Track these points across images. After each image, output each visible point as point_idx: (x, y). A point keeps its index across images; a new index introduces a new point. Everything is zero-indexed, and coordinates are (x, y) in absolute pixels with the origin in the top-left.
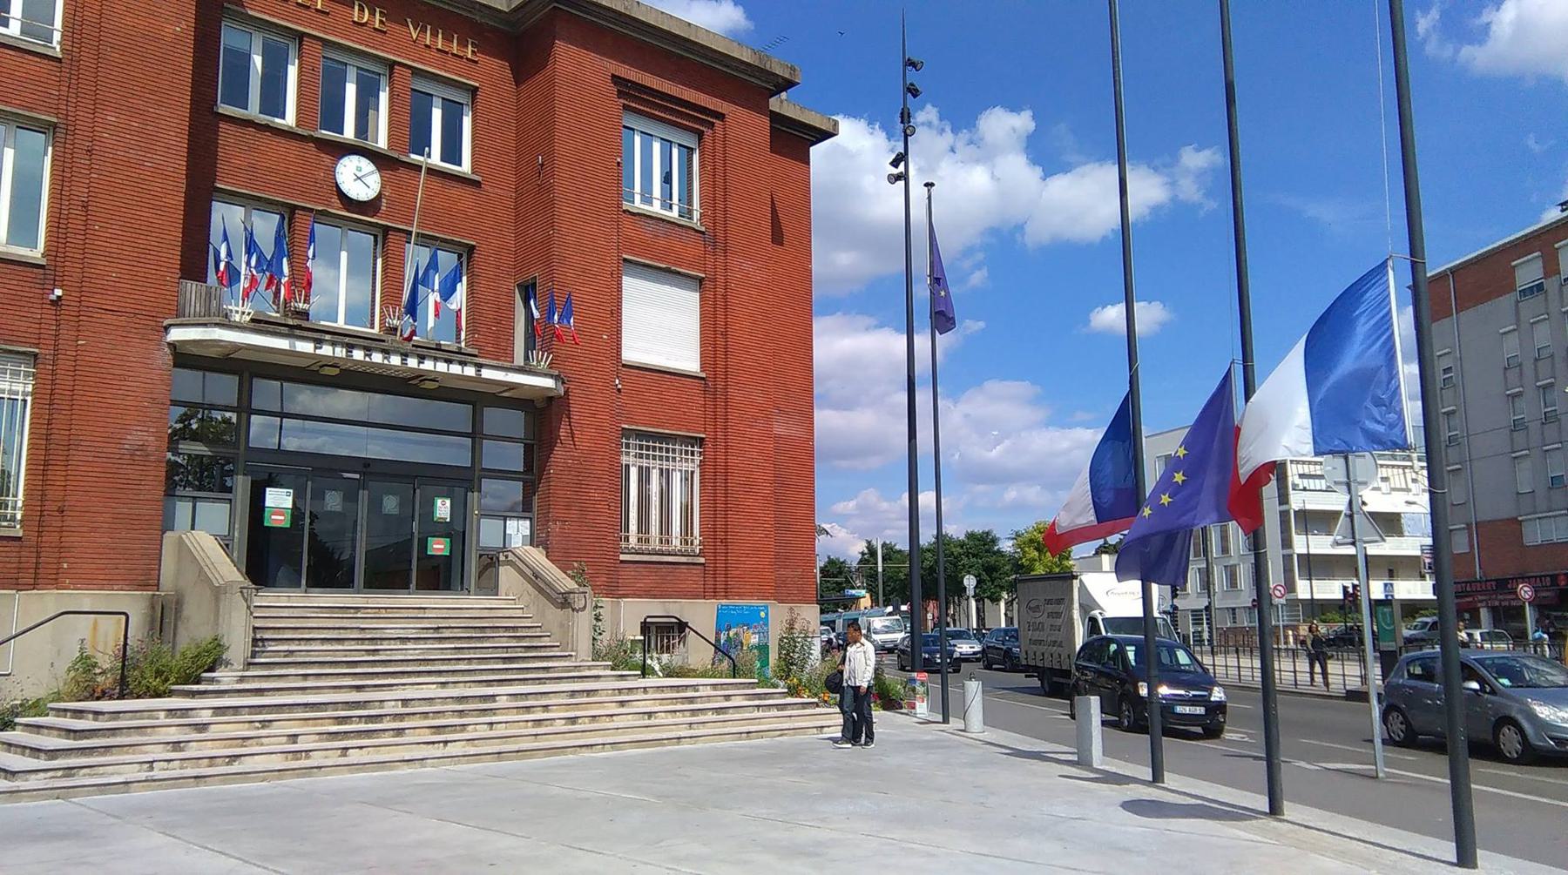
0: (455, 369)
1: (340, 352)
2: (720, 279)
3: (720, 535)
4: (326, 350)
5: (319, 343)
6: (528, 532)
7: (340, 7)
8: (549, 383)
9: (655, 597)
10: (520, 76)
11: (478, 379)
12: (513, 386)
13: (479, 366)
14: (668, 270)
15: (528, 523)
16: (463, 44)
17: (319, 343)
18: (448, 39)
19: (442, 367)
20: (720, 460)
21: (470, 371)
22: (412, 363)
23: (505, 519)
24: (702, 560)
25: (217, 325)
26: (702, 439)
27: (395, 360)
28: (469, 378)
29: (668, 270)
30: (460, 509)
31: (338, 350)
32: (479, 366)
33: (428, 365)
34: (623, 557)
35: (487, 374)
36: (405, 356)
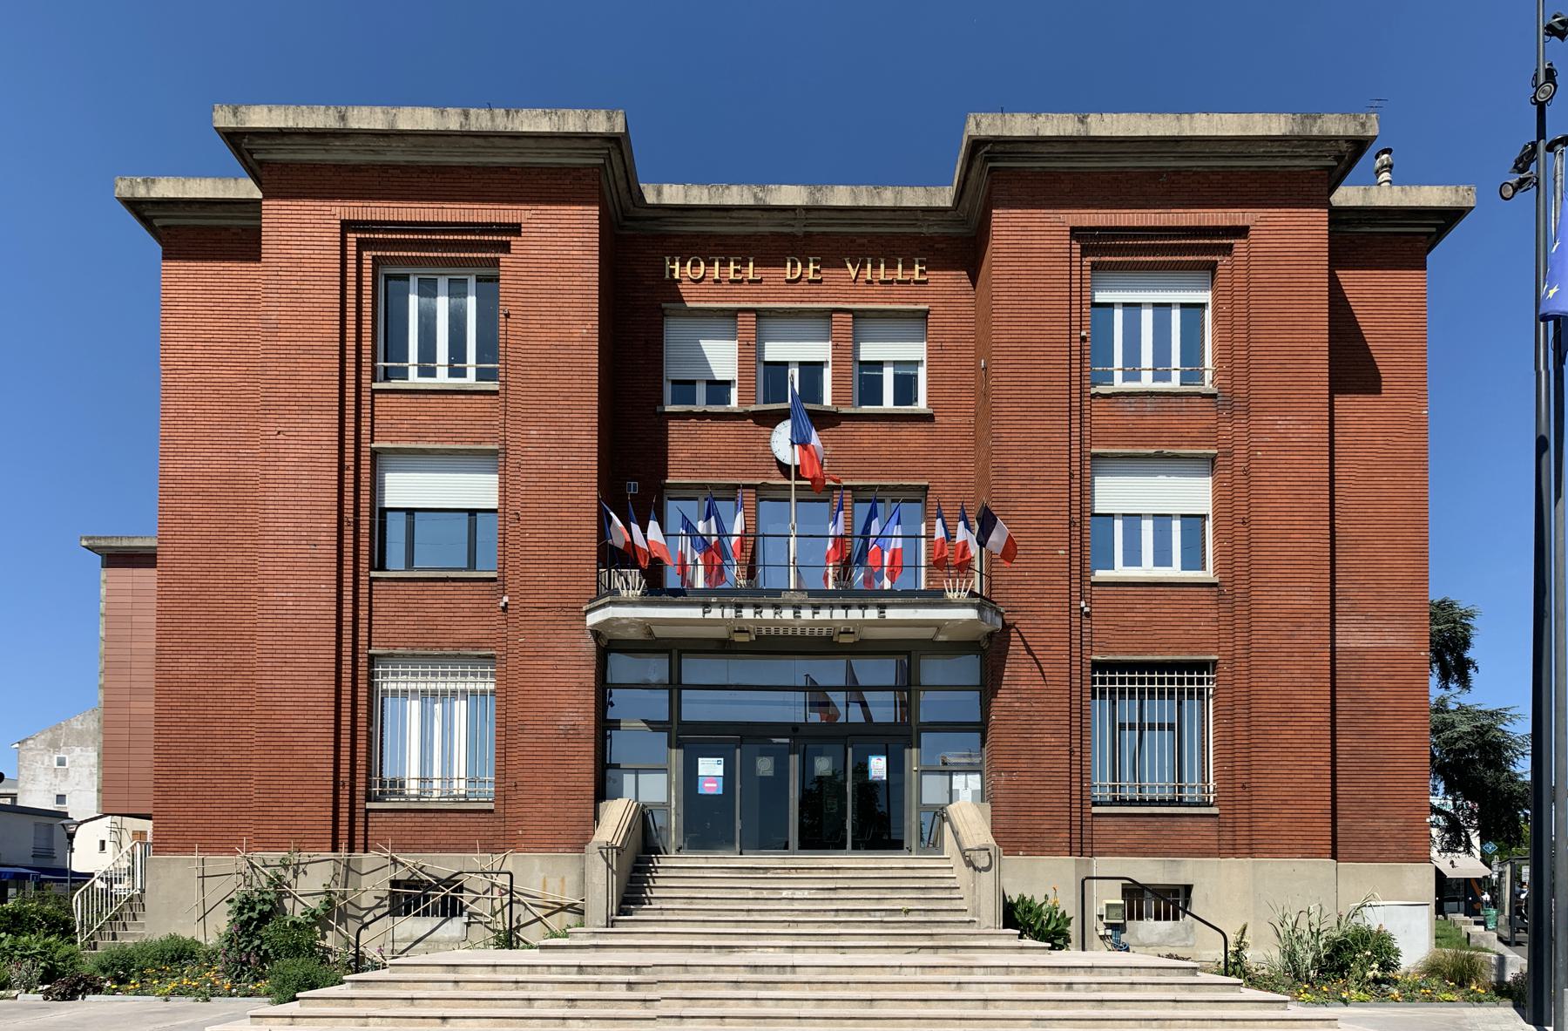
0: (855, 614)
1: (729, 613)
2: (1240, 452)
3: (1242, 777)
4: (715, 613)
5: (707, 606)
6: (979, 787)
7: (772, 270)
8: (971, 614)
9: (1145, 854)
10: (974, 279)
11: (882, 623)
12: (938, 625)
13: (882, 607)
14: (1160, 456)
15: (978, 777)
16: (908, 266)
17: (707, 606)
18: (891, 266)
19: (839, 614)
20: (1242, 684)
21: (872, 614)
22: (806, 614)
23: (951, 773)
24: (1215, 810)
25: (611, 603)
26: (1215, 662)
27: (788, 614)
28: (871, 623)
29: (1160, 456)
30: (895, 767)
31: (727, 611)
32: (882, 607)
33: (824, 615)
34: (1095, 810)
35: (891, 614)
36: (797, 608)
